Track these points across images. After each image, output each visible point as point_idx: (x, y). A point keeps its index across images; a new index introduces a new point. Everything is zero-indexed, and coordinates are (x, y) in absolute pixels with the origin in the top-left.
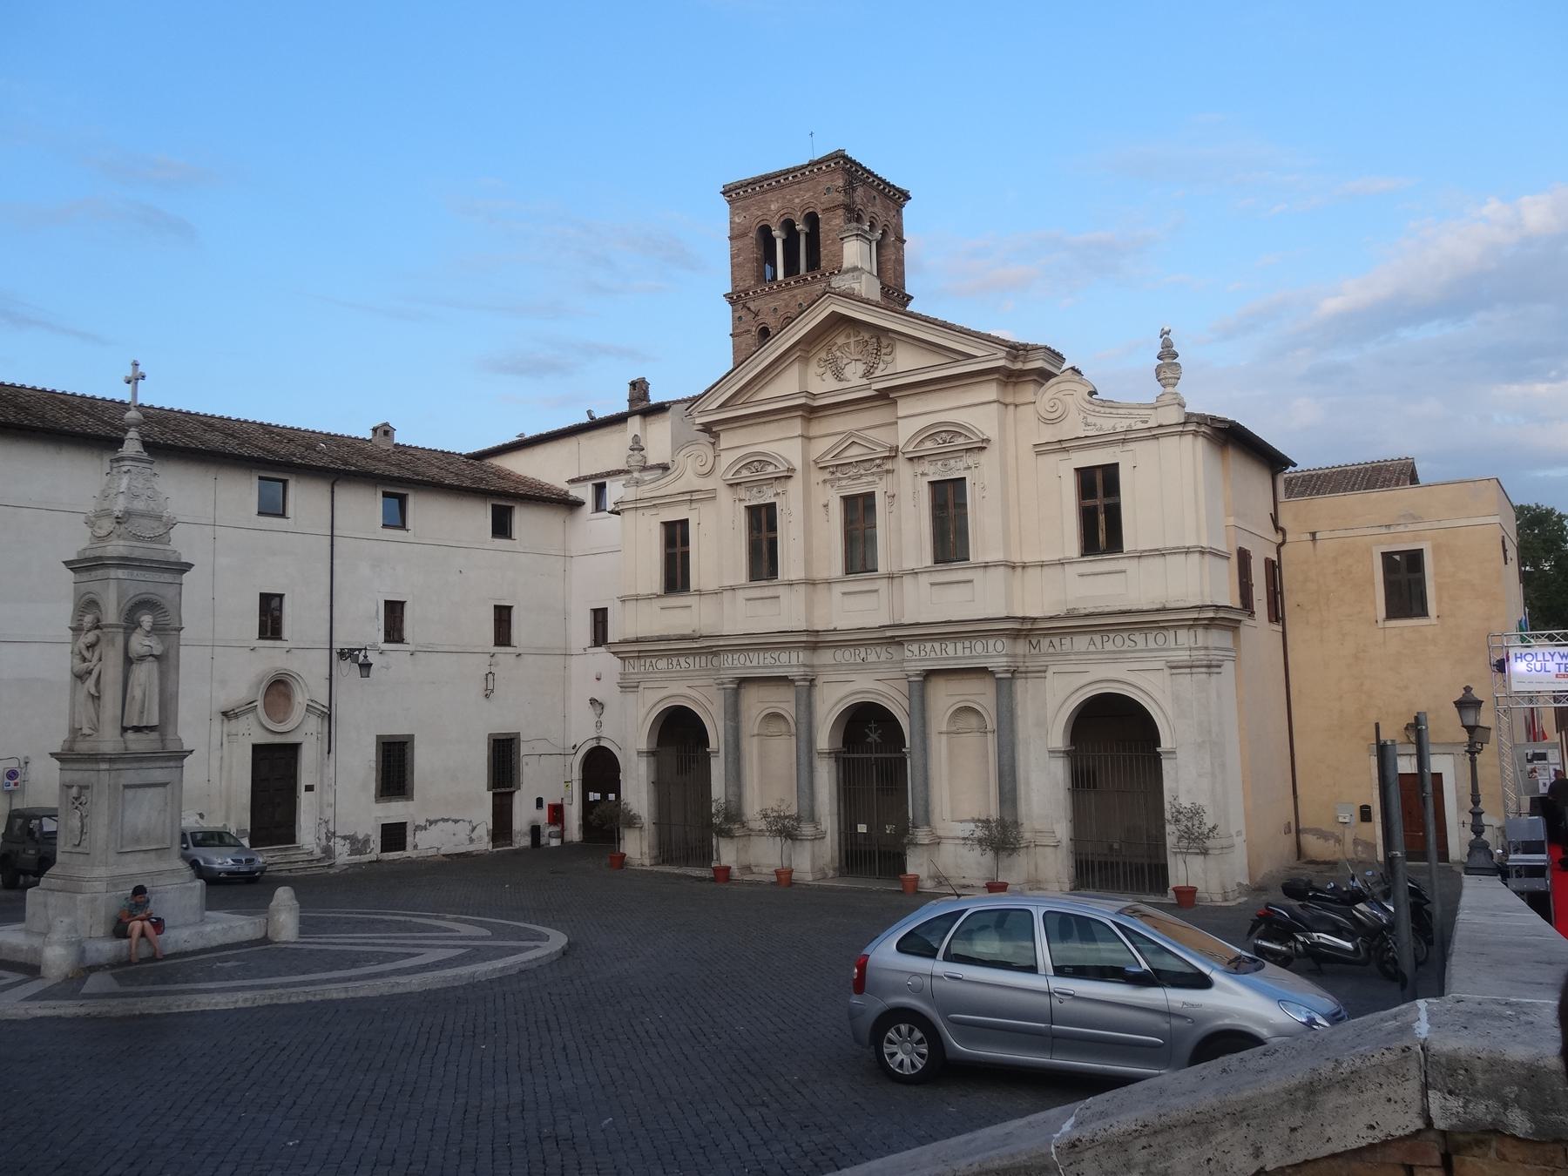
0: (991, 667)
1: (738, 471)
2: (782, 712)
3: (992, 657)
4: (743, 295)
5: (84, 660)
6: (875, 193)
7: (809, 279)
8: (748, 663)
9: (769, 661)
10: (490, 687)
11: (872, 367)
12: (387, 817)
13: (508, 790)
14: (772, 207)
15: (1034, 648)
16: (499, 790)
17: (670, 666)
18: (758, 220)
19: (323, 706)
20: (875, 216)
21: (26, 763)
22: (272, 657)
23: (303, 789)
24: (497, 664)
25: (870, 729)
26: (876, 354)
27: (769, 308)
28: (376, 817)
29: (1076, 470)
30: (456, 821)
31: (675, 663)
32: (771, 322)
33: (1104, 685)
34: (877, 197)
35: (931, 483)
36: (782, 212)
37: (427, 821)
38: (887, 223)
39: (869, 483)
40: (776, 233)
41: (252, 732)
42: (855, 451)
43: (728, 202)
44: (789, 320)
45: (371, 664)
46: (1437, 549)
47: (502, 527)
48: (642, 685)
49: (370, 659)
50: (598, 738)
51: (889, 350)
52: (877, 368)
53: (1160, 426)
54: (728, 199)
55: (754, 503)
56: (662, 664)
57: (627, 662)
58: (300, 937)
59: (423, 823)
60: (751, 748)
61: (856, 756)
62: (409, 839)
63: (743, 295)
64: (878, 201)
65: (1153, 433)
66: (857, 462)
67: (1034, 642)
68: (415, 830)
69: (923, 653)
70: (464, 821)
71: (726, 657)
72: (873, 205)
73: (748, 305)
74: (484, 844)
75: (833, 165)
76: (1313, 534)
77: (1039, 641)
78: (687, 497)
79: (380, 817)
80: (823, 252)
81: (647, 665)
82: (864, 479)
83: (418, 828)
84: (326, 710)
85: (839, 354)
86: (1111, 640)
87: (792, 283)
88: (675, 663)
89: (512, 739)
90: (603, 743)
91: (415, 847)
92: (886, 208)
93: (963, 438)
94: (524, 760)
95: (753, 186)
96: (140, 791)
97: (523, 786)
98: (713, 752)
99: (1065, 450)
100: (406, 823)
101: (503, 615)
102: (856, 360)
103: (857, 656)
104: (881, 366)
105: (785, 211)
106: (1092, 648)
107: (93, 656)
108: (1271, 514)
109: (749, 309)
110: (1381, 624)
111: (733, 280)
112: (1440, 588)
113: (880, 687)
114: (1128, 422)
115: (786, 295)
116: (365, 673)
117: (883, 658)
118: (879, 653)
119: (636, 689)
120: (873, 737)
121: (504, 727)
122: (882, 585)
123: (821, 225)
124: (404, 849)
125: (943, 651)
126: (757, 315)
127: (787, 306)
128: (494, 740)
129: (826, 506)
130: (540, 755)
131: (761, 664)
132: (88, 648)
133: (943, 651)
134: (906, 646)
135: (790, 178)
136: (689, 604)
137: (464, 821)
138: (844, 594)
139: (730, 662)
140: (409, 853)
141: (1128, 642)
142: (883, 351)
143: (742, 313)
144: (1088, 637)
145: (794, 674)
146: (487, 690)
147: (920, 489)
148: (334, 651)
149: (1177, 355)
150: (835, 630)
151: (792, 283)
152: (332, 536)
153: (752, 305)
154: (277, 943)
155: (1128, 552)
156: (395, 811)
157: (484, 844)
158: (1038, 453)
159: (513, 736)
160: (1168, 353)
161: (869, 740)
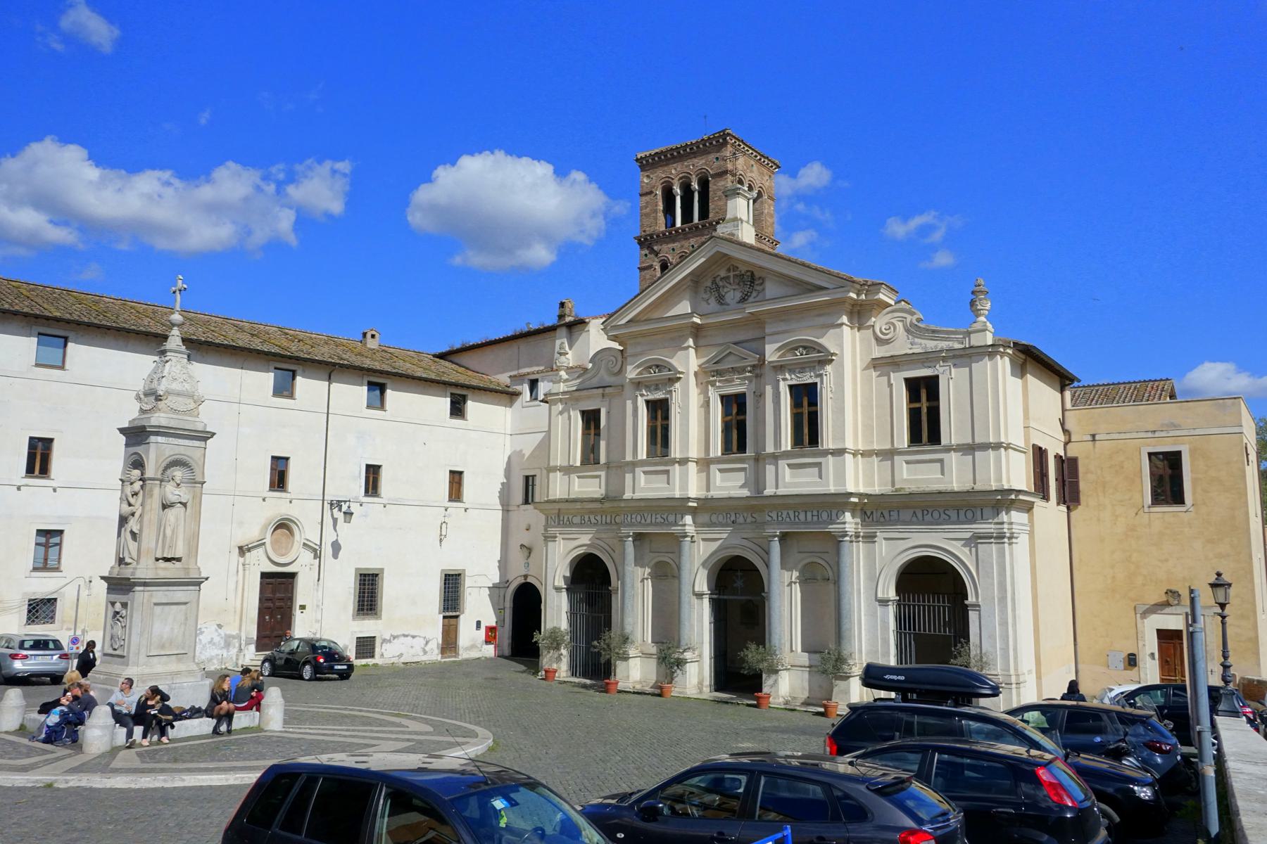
0: (833, 532)
1: (640, 373)
5: (130, 505)
6: (752, 162)
7: (700, 226)
8: (643, 521)
9: (659, 520)
10: (444, 533)
11: (746, 295)
12: (361, 632)
13: (454, 614)
14: (673, 171)
15: (869, 518)
16: (447, 614)
17: (583, 522)
18: (663, 180)
19: (316, 545)
20: (752, 179)
21: (90, 581)
22: (279, 505)
23: (298, 607)
24: (450, 516)
25: (737, 576)
26: (751, 285)
28: (352, 632)
30: (414, 637)
32: (672, 259)
34: (754, 165)
36: (681, 175)
37: (392, 635)
38: (761, 185)
41: (260, 563)
42: (731, 358)
43: (640, 166)
44: (683, 257)
45: (353, 513)
46: (1193, 452)
47: (457, 410)
49: (352, 510)
50: (526, 576)
51: (761, 281)
52: (750, 296)
54: (639, 164)
55: (651, 397)
57: (549, 518)
58: (284, 727)
59: (388, 638)
61: (725, 597)
62: (377, 650)
64: (755, 168)
65: (967, 352)
66: (732, 368)
67: (869, 514)
68: (382, 643)
69: (780, 519)
70: (420, 637)
72: (752, 171)
74: (434, 655)
75: (721, 141)
76: (1093, 436)
77: (872, 513)
78: (600, 391)
79: (355, 632)
80: (711, 206)
81: (565, 520)
83: (384, 641)
84: (317, 548)
85: (721, 284)
86: (930, 514)
89: (459, 575)
90: (528, 580)
91: (382, 655)
92: (762, 174)
94: (467, 591)
95: (659, 155)
96: (167, 608)
97: (467, 611)
100: (374, 637)
101: (456, 478)
102: (734, 290)
104: (754, 294)
105: (683, 174)
106: (914, 519)
107: (136, 502)
108: (1060, 419)
109: (653, 249)
110: (1146, 510)
111: (642, 226)
112: (1195, 482)
114: (947, 343)
116: (348, 519)
120: (739, 583)
121: (453, 566)
123: (710, 185)
124: (373, 657)
128: (446, 575)
129: (707, 404)
130: (480, 587)
131: (653, 521)
132: (133, 495)
135: (688, 150)
137: (420, 637)
139: (629, 519)
140: (377, 660)
141: (942, 513)
142: (757, 282)
143: (647, 252)
144: (912, 511)
146: (441, 535)
148: (325, 502)
152: (328, 413)
153: (655, 248)
154: (266, 731)
155: (944, 446)
156: (367, 627)
157: (434, 655)
159: (459, 572)
161: (735, 585)
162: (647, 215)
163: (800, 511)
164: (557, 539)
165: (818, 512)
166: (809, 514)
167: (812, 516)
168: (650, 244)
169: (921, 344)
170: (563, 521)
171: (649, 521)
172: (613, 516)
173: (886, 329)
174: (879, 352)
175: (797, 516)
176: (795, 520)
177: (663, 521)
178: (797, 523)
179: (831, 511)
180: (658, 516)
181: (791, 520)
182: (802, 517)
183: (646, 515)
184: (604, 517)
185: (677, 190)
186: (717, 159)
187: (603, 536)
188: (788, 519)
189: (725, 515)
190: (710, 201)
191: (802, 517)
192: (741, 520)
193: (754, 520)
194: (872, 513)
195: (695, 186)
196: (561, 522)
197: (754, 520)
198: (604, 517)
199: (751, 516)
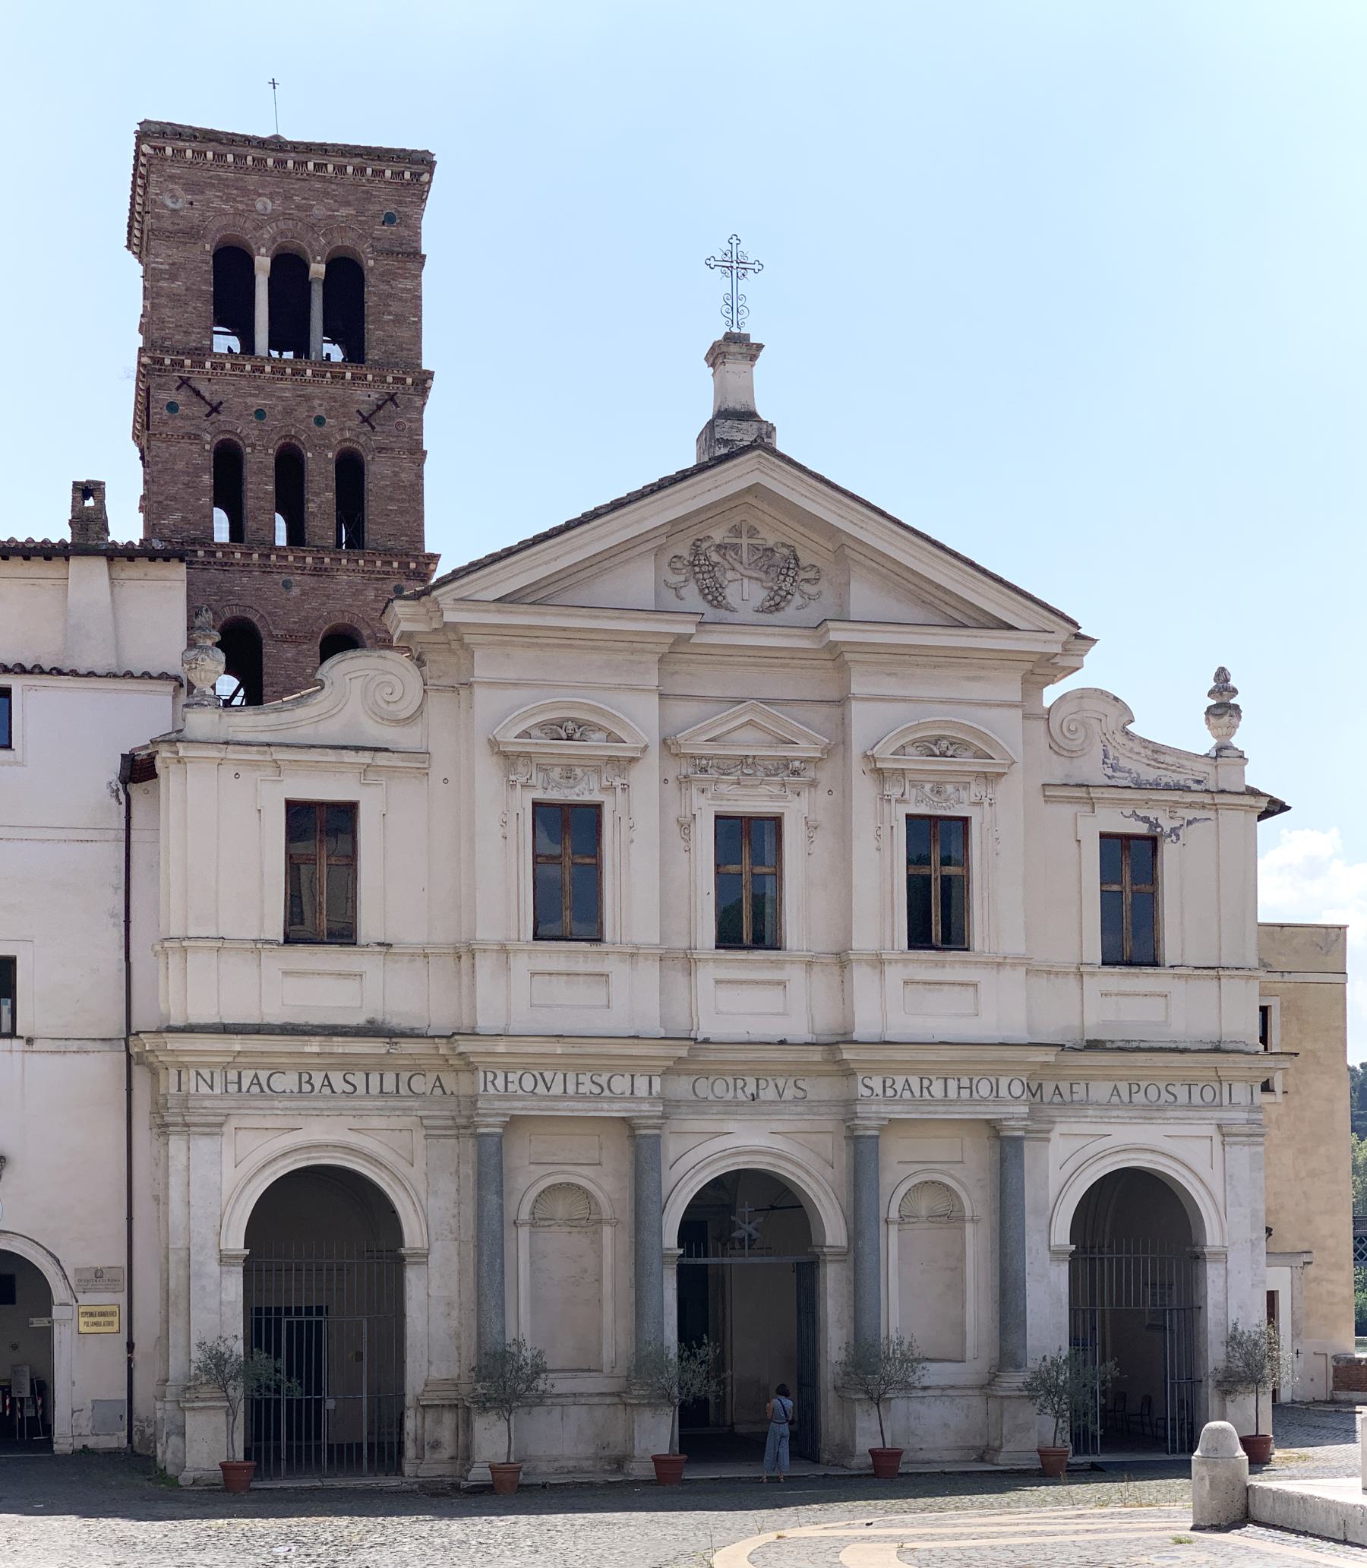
2: (583, 1182)
3: (1005, 1104)
4: (188, 362)
8: (541, 1089)
9: (586, 1088)
17: (306, 1088)
27: (247, 407)
29: (1103, 836)
31: (318, 1079)
33: (1132, 1155)
35: (908, 817)
39: (772, 797)
40: (263, 265)
48: (234, 1122)
53: (1223, 791)
56: (286, 1082)
60: (521, 1246)
63: (188, 362)
69: (890, 1092)
71: (490, 1077)
73: (193, 383)
82: (764, 789)
87: (309, 372)
88: (318, 1079)
93: (969, 753)
98: (412, 1255)
99: (1091, 803)
103: (739, 1091)
109: (198, 393)
113: (780, 1144)
115: (286, 389)
117: (789, 1094)
118: (781, 1085)
119: (217, 1130)
122: (795, 975)
123: (371, 280)
125: (925, 1091)
126: (215, 409)
127: (288, 412)
129: (686, 827)
131: (571, 1089)
133: (925, 1091)
134: (860, 1078)
136: (356, 970)
138: (718, 982)
143: (181, 397)
145: (646, 1114)
147: (894, 824)
149: (1235, 691)
150: (706, 1041)
151: (309, 372)
158: (1048, 799)
160: (1222, 687)
162: (175, 299)
163: (933, 1078)
164: (225, 1129)
165: (971, 1080)
166: (952, 1085)
167: (959, 1088)
168: (189, 378)
169: (1129, 772)
170: (239, 1083)
171: (557, 1089)
172: (405, 1076)
173: (1069, 730)
174: (1058, 770)
175: (928, 1088)
176: (921, 1096)
177: (597, 1090)
178: (929, 1103)
179: (997, 1080)
180: (584, 1078)
181: (914, 1096)
182: (937, 1089)
183: (548, 1076)
184: (374, 1079)
185: (263, 265)
186: (390, 219)
187: (376, 1122)
188: (907, 1095)
189: (731, 1081)
190: (369, 319)
191: (937, 1089)
192: (769, 1094)
193: (801, 1094)
194: (1040, 1085)
195: (318, 269)
196: (233, 1088)
197: (801, 1094)
198: (374, 1079)
199: (795, 1085)
